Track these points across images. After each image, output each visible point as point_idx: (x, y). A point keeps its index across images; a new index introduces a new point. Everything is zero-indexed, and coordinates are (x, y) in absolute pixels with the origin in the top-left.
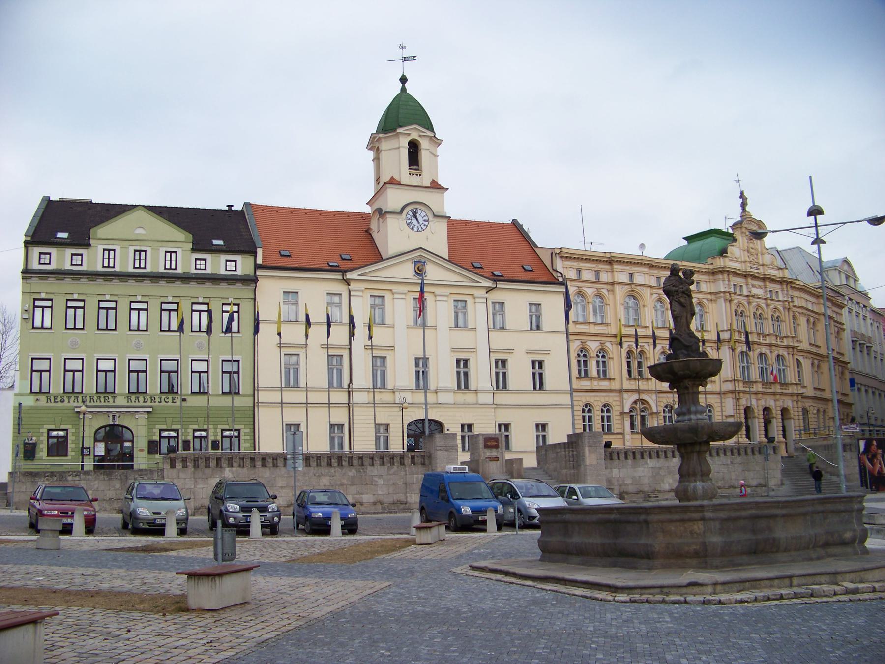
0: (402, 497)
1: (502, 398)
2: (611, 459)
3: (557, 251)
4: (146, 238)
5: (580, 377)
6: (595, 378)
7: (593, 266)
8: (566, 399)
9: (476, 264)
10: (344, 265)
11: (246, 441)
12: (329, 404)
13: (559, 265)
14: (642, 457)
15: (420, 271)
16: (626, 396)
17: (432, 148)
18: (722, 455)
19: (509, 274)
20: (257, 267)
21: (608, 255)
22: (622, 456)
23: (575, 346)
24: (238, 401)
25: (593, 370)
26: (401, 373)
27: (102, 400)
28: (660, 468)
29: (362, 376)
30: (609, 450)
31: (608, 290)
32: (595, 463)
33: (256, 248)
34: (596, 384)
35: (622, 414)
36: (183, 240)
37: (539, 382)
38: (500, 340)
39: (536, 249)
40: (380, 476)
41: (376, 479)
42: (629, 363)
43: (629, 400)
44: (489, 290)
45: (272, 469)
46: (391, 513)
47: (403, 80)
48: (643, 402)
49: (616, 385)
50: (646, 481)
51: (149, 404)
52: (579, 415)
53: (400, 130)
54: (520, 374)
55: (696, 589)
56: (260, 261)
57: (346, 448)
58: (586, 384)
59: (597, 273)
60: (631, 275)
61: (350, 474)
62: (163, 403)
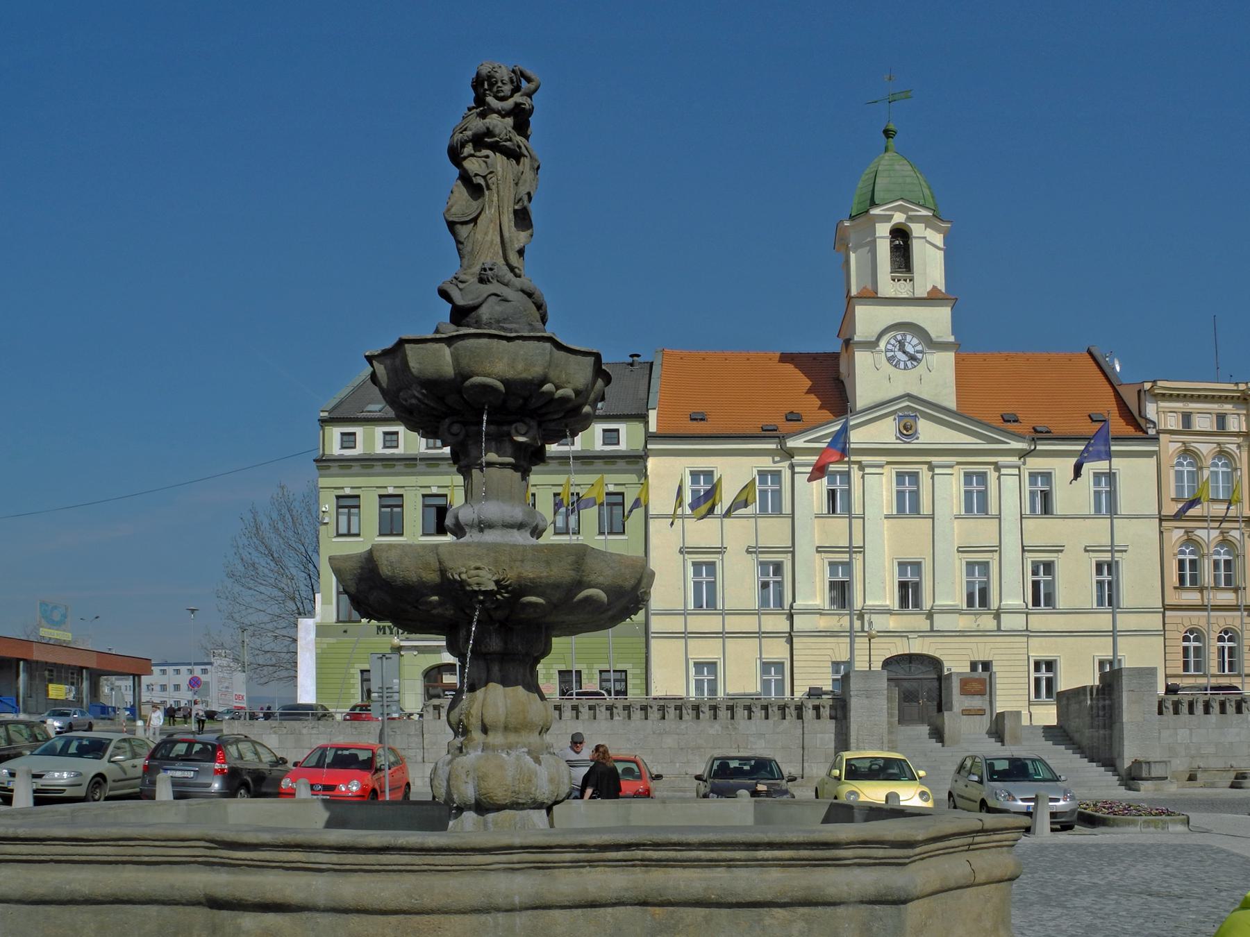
1: (1040, 621)
8: (1155, 621)
10: (785, 427)
11: (635, 686)
15: (907, 431)
26: (877, 588)
29: (812, 592)
37: (1108, 595)
38: (1041, 531)
44: (1024, 454)
53: (876, 211)
54: (1075, 583)
59: (1221, 419)
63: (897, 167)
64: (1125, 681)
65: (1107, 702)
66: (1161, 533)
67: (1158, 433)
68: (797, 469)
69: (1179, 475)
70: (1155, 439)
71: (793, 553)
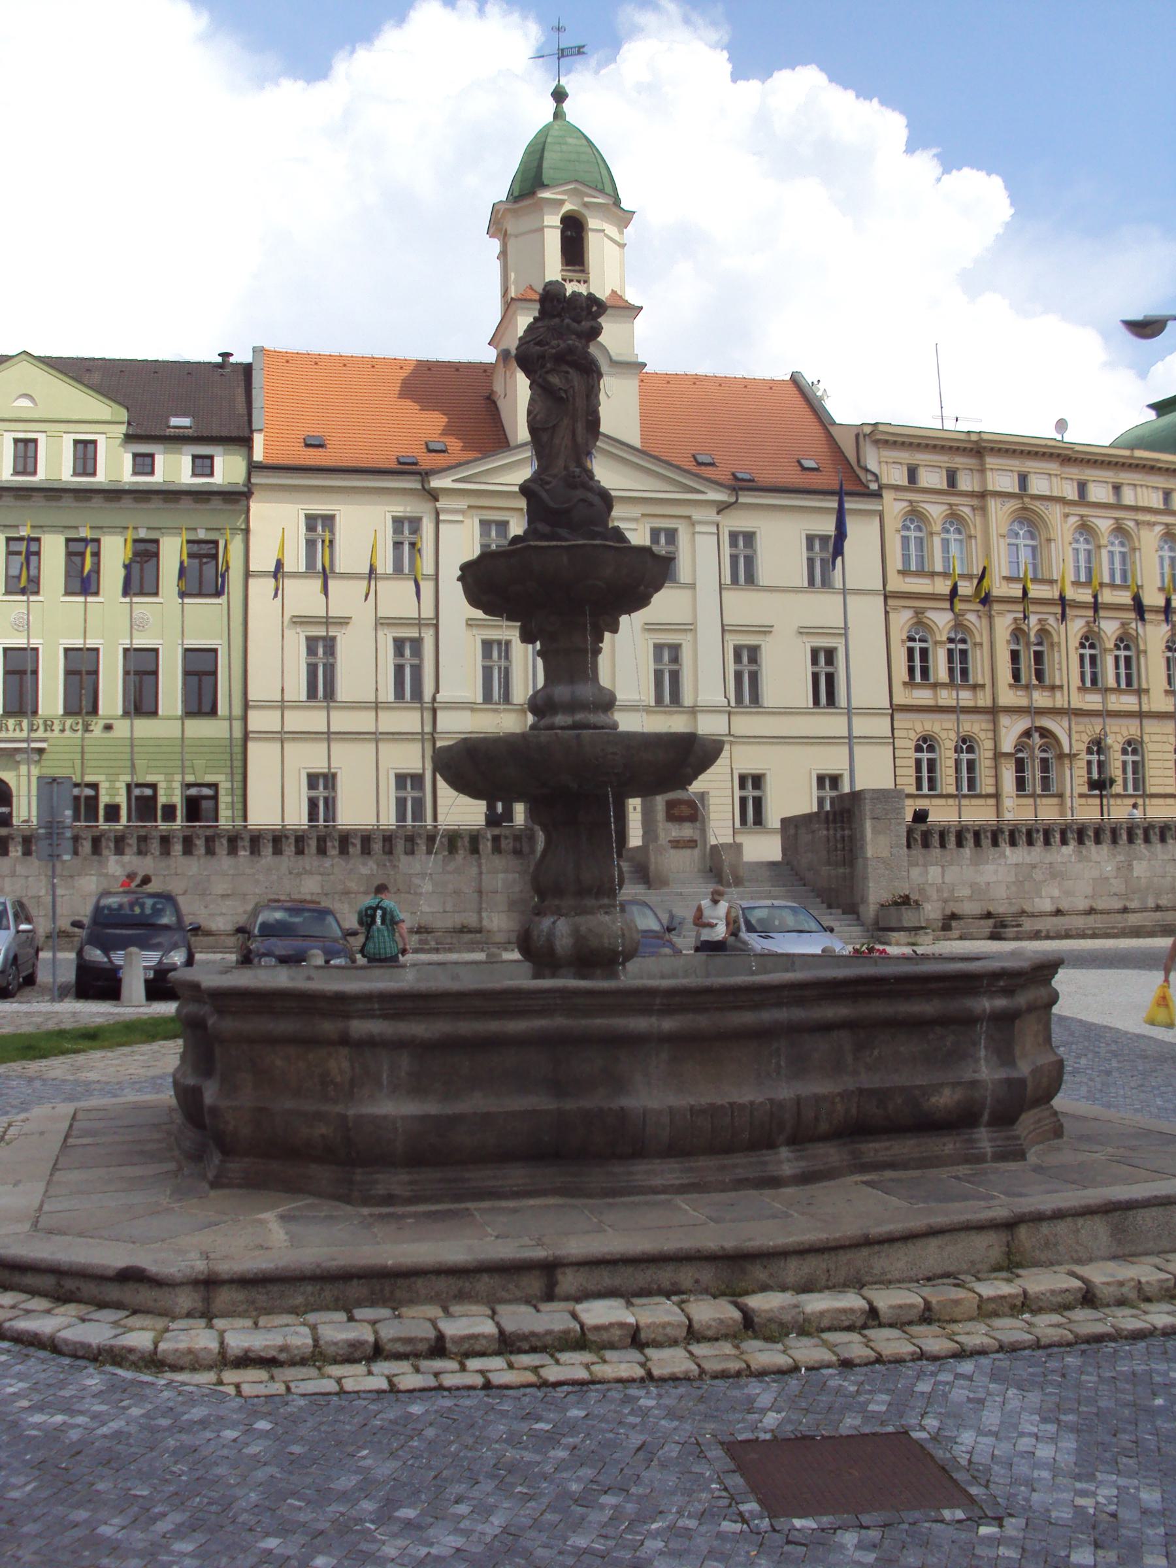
0: (471, 920)
2: (926, 845)
3: (868, 430)
4: (36, 416)
5: (910, 683)
6: (943, 685)
7: (943, 460)
9: (701, 459)
10: (427, 461)
12: (329, 733)
13: (872, 459)
14: (995, 843)
16: (1004, 720)
17: (611, 230)
18: (1140, 841)
19: (765, 476)
20: (253, 467)
21: (974, 438)
22: (952, 840)
23: (902, 619)
24: (200, 728)
25: (940, 670)
27: (11, 727)
28: (1034, 866)
30: (923, 827)
31: (974, 509)
32: (885, 854)
33: (252, 432)
34: (946, 697)
35: (998, 755)
36: (108, 418)
37: (826, 690)
38: (745, 607)
39: (832, 429)
40: (423, 875)
41: (416, 881)
42: (1015, 656)
43: (1011, 731)
44: (722, 508)
45: (202, 860)
46: (437, 950)
47: (559, 96)
48: (1045, 733)
49: (984, 700)
50: (1001, 892)
51: (40, 733)
52: (909, 756)
55: (144, 1296)
56: (258, 456)
57: (429, 821)
58: (923, 696)
60: (1023, 479)
61: (365, 871)
62: (68, 733)
63: (570, 141)
64: (868, 807)
65: (847, 832)
66: (887, 613)
67: (880, 487)
68: (441, 517)
69: (905, 540)
70: (877, 495)
71: (436, 626)
